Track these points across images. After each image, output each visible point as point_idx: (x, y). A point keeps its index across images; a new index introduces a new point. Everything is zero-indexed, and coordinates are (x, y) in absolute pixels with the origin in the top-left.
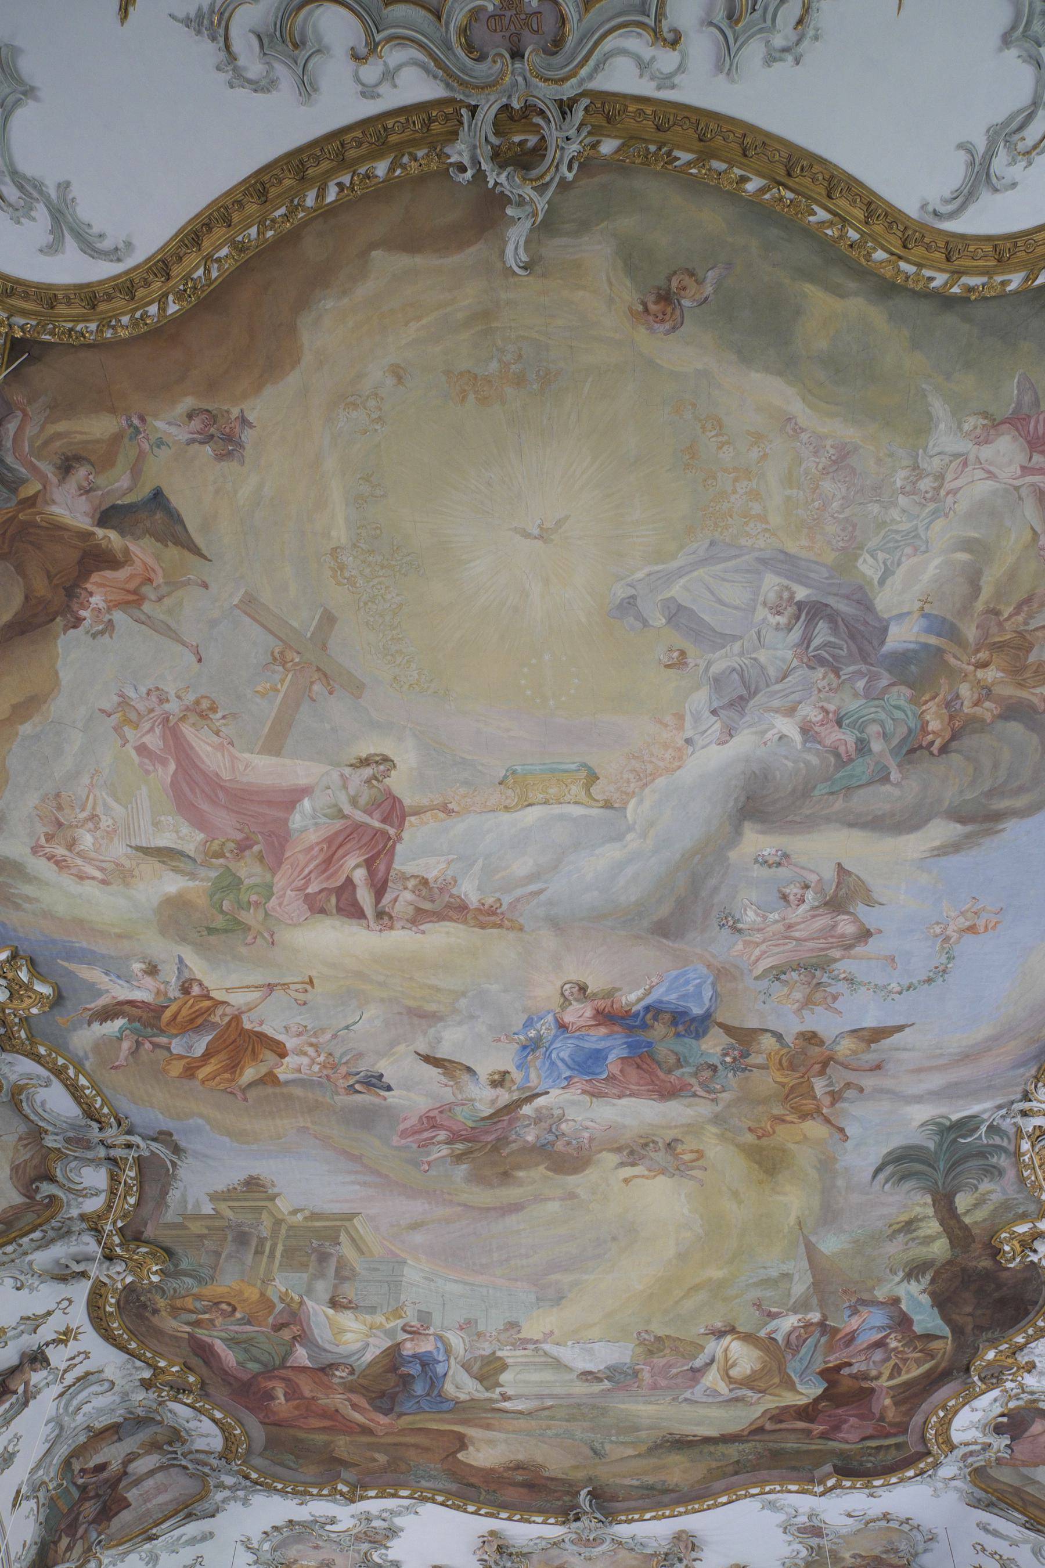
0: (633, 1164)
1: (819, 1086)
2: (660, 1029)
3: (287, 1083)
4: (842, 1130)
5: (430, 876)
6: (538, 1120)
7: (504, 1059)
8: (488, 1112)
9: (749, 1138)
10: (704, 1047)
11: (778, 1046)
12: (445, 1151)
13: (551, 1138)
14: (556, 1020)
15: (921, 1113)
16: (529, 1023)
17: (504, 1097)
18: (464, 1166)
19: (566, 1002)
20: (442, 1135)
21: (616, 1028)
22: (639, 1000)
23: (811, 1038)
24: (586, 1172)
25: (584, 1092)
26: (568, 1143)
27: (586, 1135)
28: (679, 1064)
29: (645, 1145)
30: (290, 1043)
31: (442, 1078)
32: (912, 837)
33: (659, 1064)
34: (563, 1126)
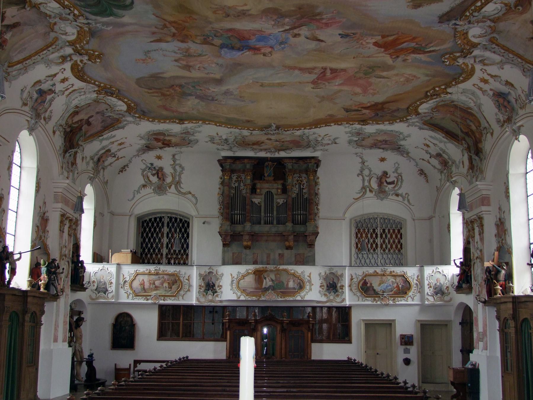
0: (243, 10)
1: (173, 30)
2: (238, 46)
3: (379, 36)
4: (157, 17)
5: (308, 74)
6: (284, 25)
7: (293, 40)
8: (304, 27)
9: (195, 17)
10: (221, 41)
11: (194, 40)
12: (324, 16)
13: (279, 20)
14: (274, 49)
15: (126, 19)
16: (283, 48)
17: (296, 31)
18: (318, 11)
19: (270, 53)
20: (324, 21)
21: (253, 47)
22: (246, 52)
23: (182, 42)
24: (263, 8)
25: (265, 32)
26: (272, 18)
27: (263, 20)
28: (229, 38)
29: (239, 16)
30: (371, 45)
31: (318, 36)
32: (173, 75)
33: (236, 37)
34: (273, 23)
